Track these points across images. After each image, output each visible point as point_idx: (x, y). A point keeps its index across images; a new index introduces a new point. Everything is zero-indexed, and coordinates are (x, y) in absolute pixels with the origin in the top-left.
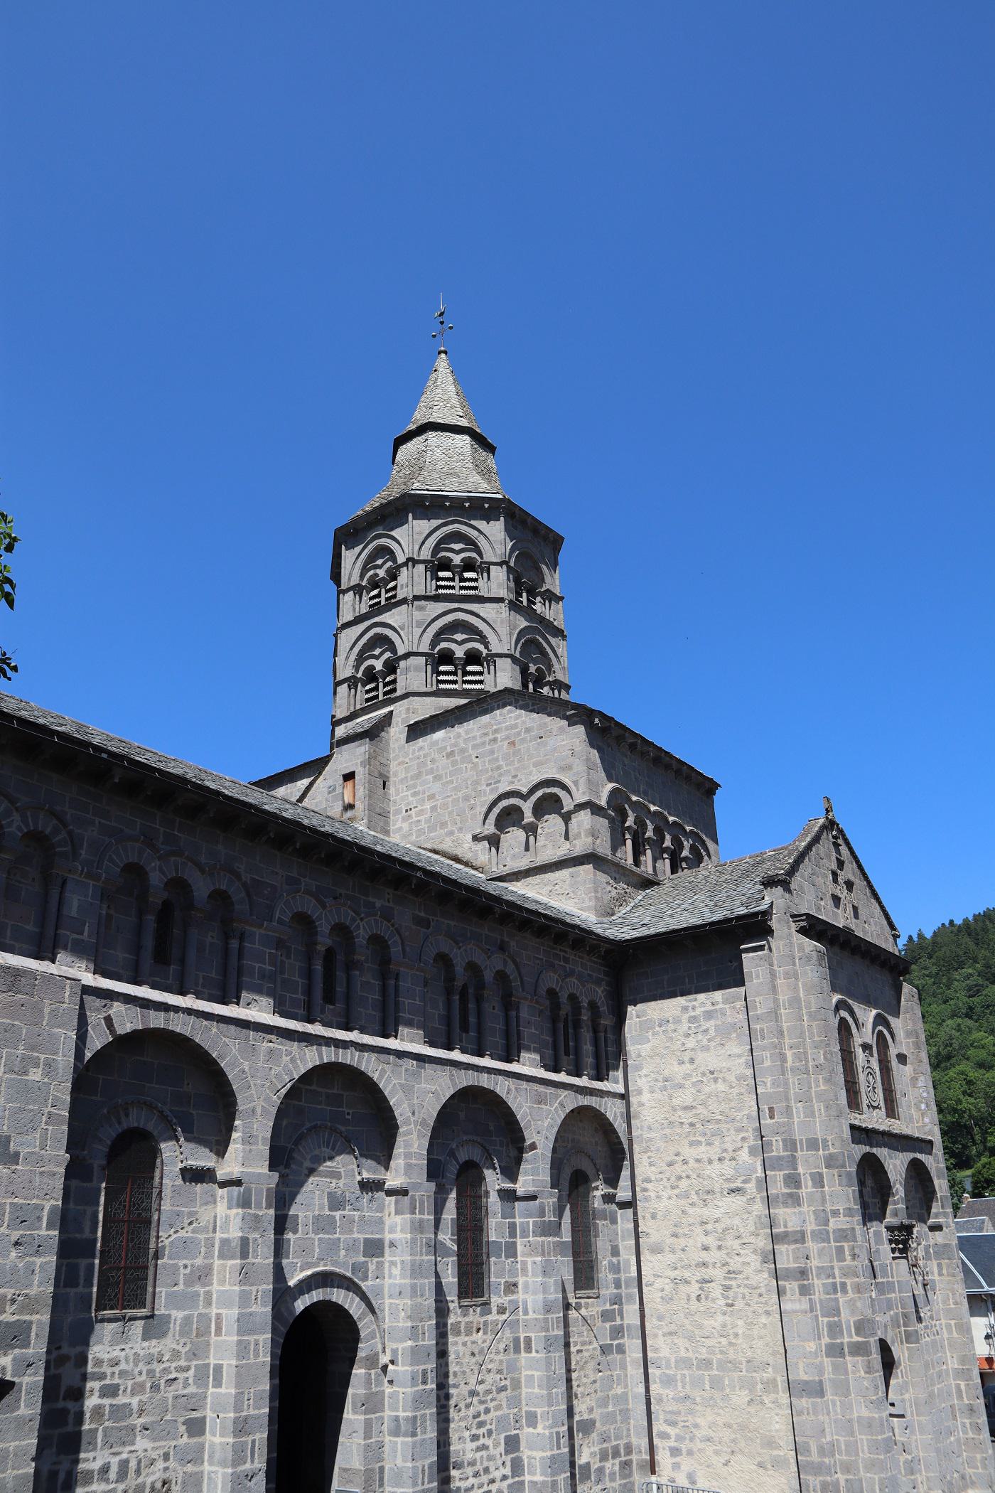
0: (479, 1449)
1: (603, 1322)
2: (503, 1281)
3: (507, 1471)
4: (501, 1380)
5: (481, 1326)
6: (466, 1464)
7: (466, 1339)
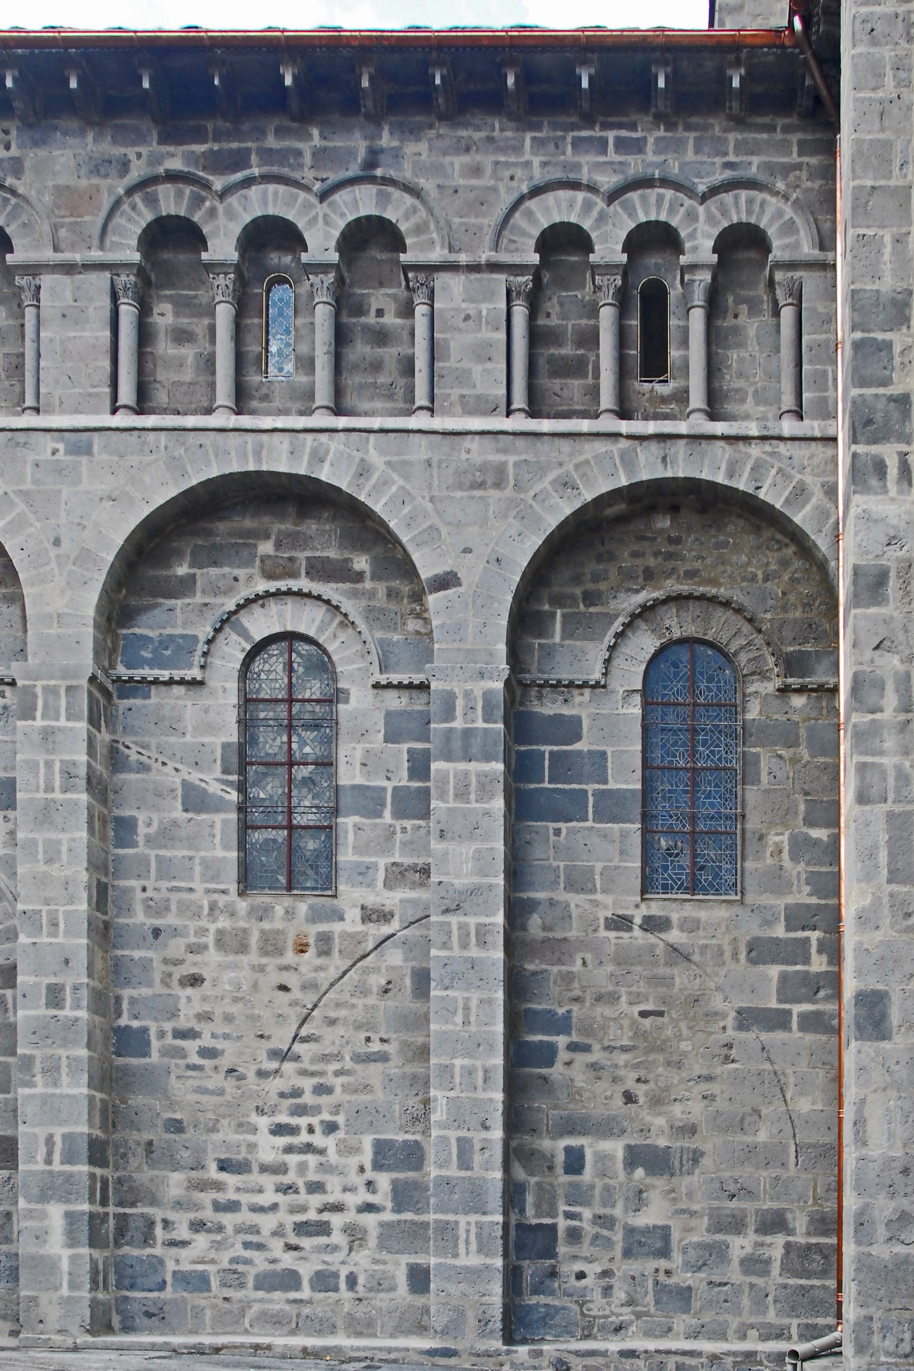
0: (289, 1150)
1: (753, 962)
2: (383, 862)
3: (382, 1197)
4: (368, 1039)
5: (311, 941)
6: (255, 1168)
7: (264, 961)
